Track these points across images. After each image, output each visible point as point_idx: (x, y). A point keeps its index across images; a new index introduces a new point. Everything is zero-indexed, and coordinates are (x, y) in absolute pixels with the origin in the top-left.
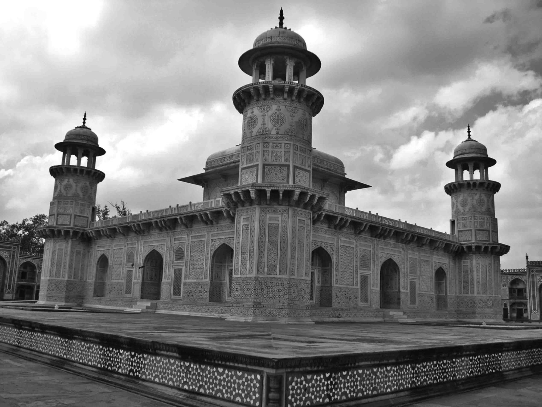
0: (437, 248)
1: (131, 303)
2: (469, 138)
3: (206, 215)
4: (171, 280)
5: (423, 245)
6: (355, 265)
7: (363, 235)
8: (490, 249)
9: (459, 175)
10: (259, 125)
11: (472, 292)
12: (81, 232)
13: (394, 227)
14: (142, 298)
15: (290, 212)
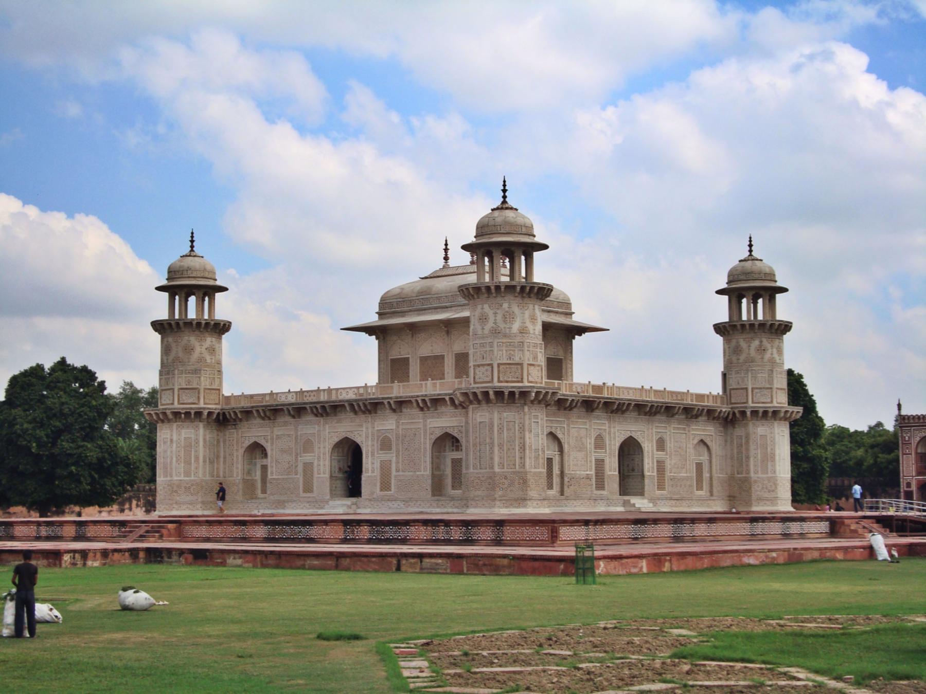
0: (696, 416)
1: (321, 503)
2: (751, 255)
3: (424, 400)
4: (377, 473)
5: (673, 416)
6: (590, 446)
7: (597, 413)
8: (770, 414)
9: (735, 307)
10: (490, 324)
11: (748, 472)
12: (217, 411)
13: (634, 400)
14: (333, 495)
15: (526, 409)
